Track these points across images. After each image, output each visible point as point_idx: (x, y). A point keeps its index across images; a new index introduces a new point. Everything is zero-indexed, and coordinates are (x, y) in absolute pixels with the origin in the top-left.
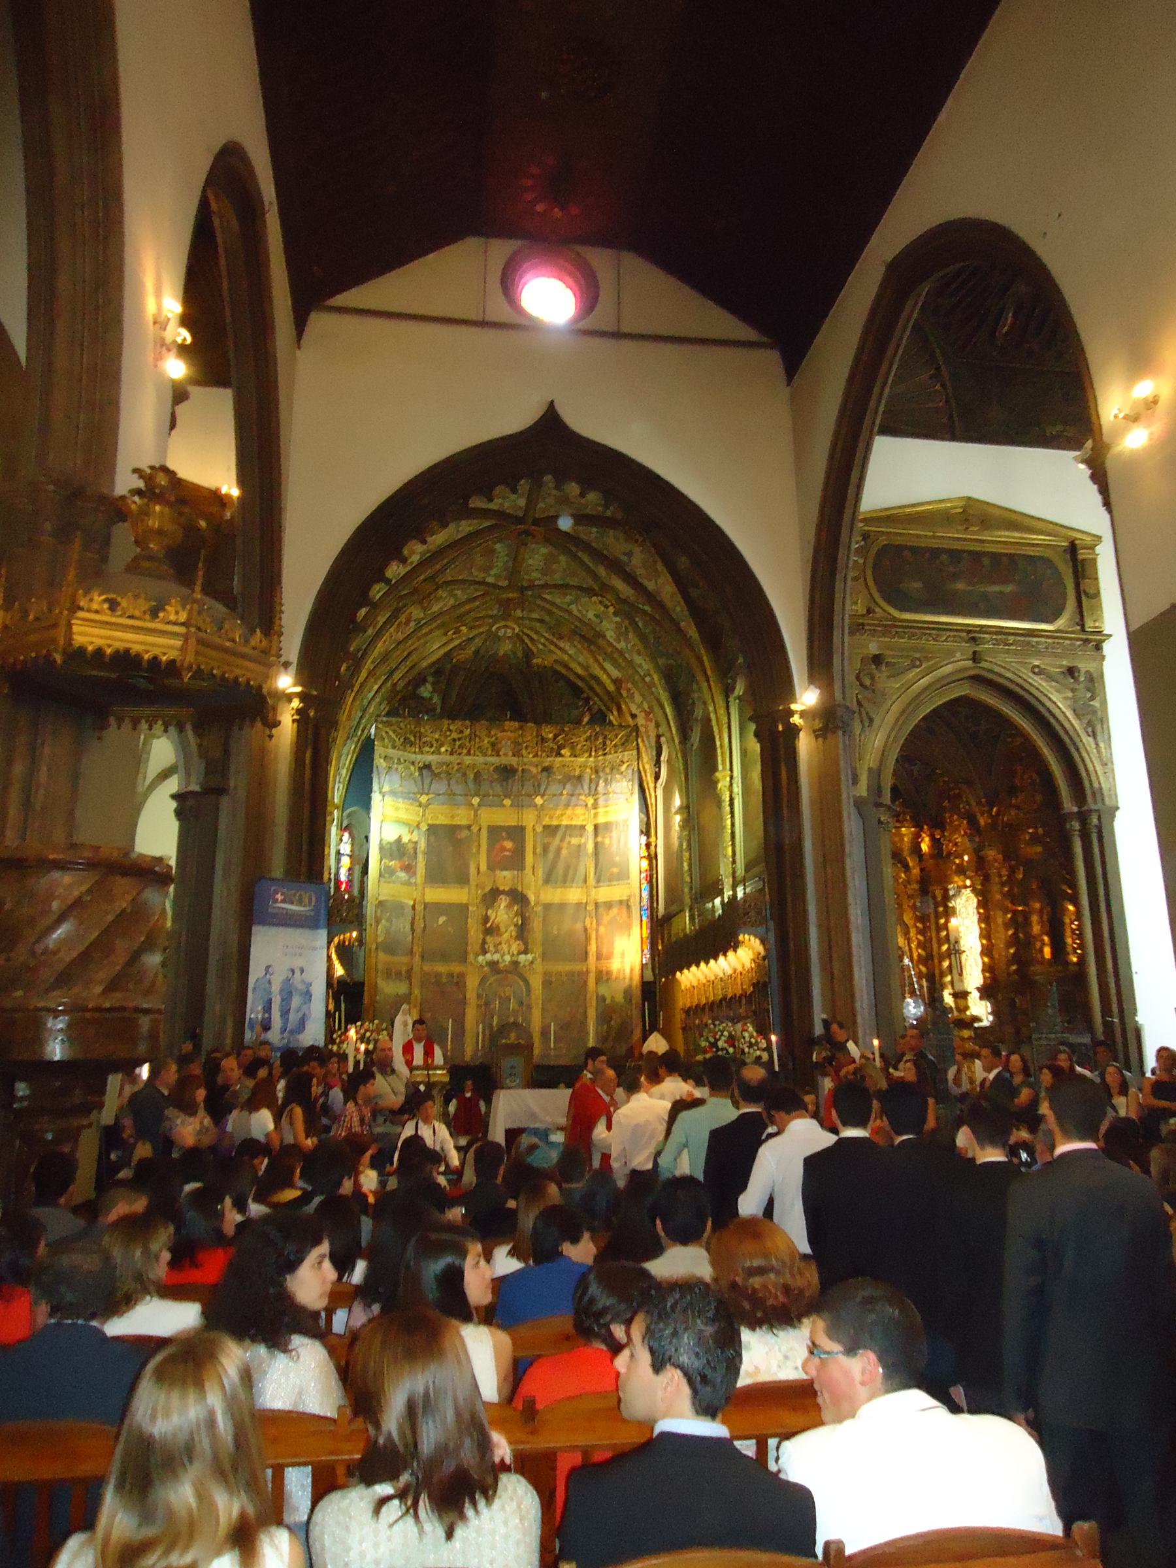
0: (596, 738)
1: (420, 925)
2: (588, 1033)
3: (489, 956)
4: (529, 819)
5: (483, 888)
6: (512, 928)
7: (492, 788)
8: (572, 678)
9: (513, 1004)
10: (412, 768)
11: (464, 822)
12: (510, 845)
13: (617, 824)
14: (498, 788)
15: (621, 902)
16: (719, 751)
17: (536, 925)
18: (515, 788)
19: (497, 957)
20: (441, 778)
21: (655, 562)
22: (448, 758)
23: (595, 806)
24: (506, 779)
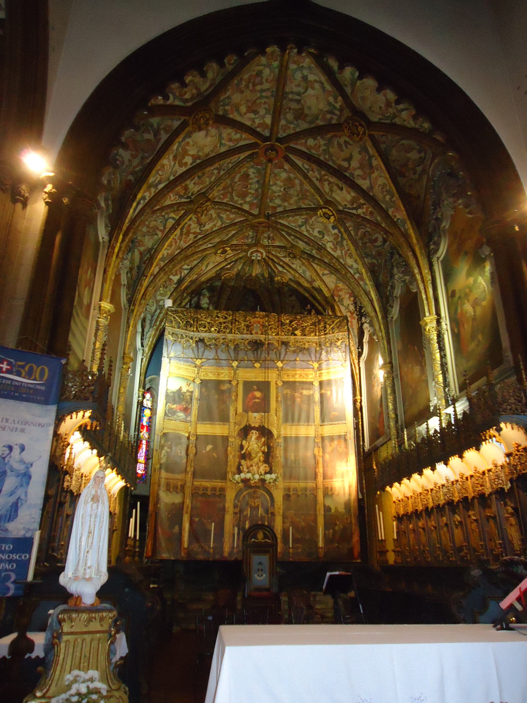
0: (319, 324)
1: (192, 450)
2: (318, 536)
3: (243, 475)
4: (272, 376)
5: (239, 425)
6: (261, 454)
7: (246, 354)
8: (301, 290)
9: (261, 511)
10: (191, 341)
11: (227, 379)
12: (259, 396)
13: (336, 381)
14: (251, 356)
15: (340, 436)
16: (425, 302)
17: (279, 453)
18: (263, 355)
19: (249, 476)
20: (211, 348)
21: (370, 157)
22: (216, 335)
23: (320, 368)
24: (256, 350)
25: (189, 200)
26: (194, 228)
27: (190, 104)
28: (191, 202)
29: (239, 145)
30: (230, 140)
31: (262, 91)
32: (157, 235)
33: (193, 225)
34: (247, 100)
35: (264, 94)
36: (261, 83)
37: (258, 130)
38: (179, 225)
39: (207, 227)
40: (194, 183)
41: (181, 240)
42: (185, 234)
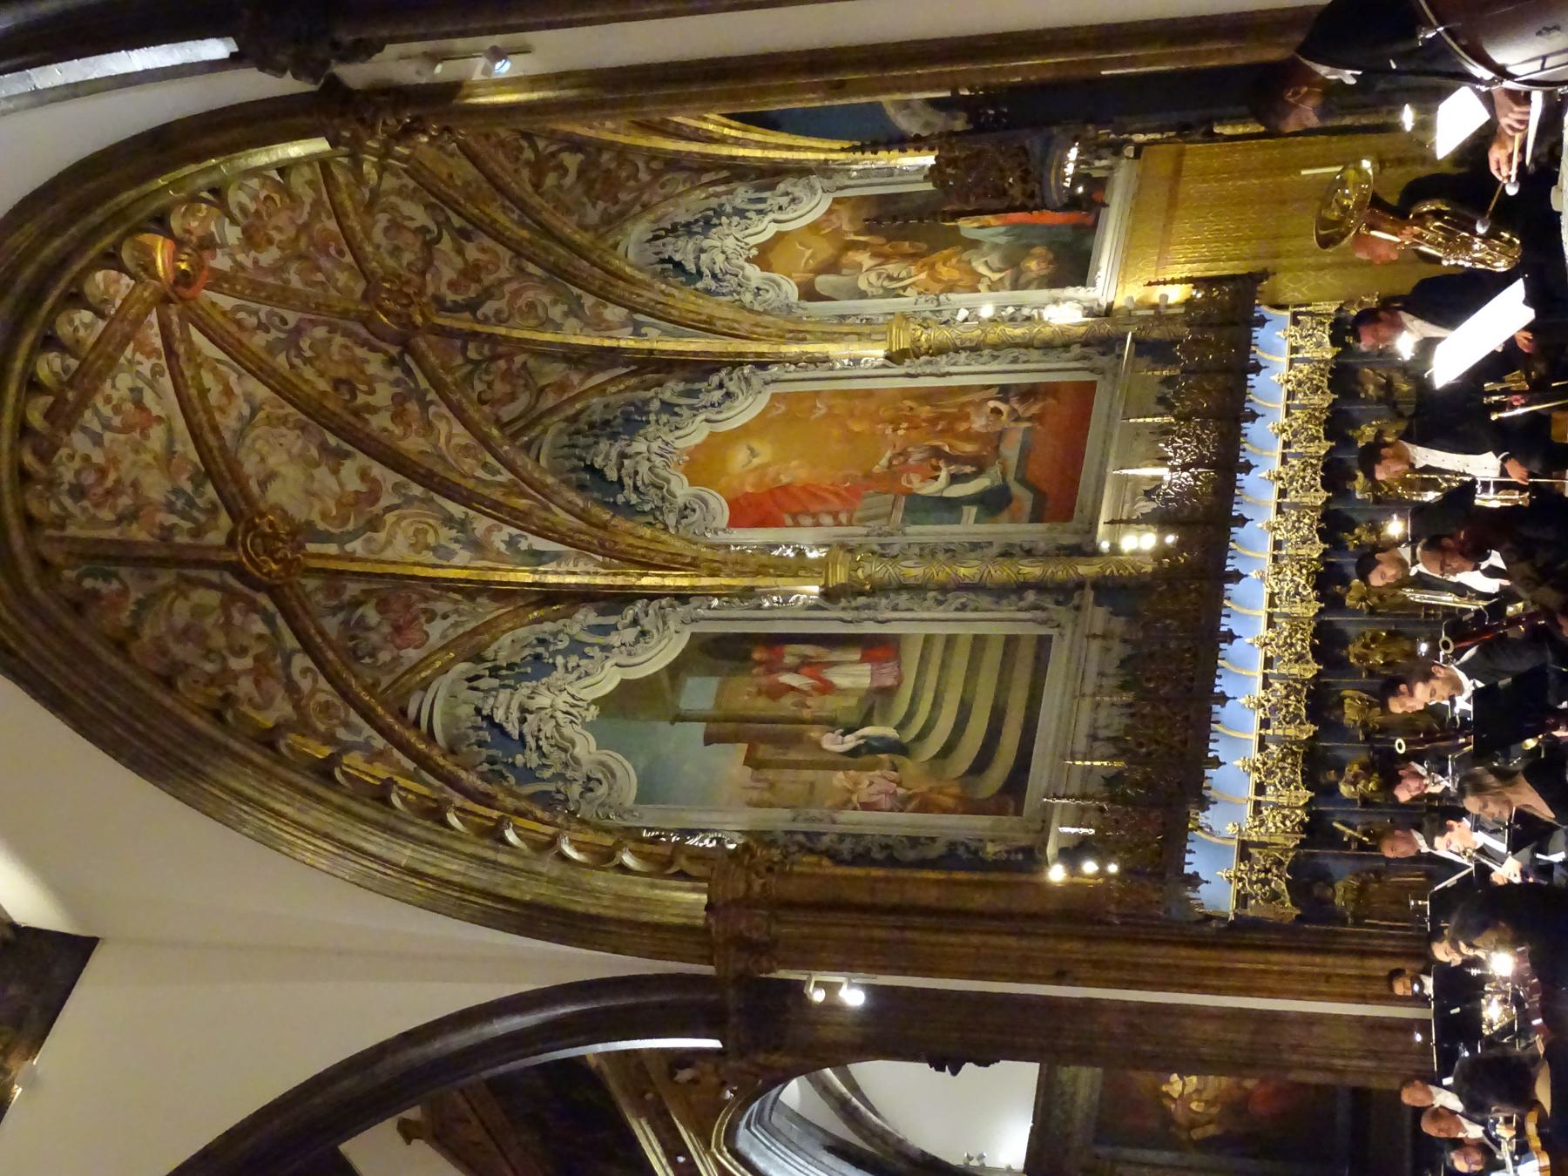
25: (408, 359)
26: (448, 262)
27: (264, 600)
28: (407, 347)
29: (221, 355)
30: (228, 392)
31: (97, 441)
32: (525, 364)
33: (448, 274)
34: (137, 452)
35: (96, 426)
36: (87, 459)
37: (158, 342)
38: (475, 335)
39: (418, 215)
40: (372, 392)
41: (501, 282)
42: (479, 281)
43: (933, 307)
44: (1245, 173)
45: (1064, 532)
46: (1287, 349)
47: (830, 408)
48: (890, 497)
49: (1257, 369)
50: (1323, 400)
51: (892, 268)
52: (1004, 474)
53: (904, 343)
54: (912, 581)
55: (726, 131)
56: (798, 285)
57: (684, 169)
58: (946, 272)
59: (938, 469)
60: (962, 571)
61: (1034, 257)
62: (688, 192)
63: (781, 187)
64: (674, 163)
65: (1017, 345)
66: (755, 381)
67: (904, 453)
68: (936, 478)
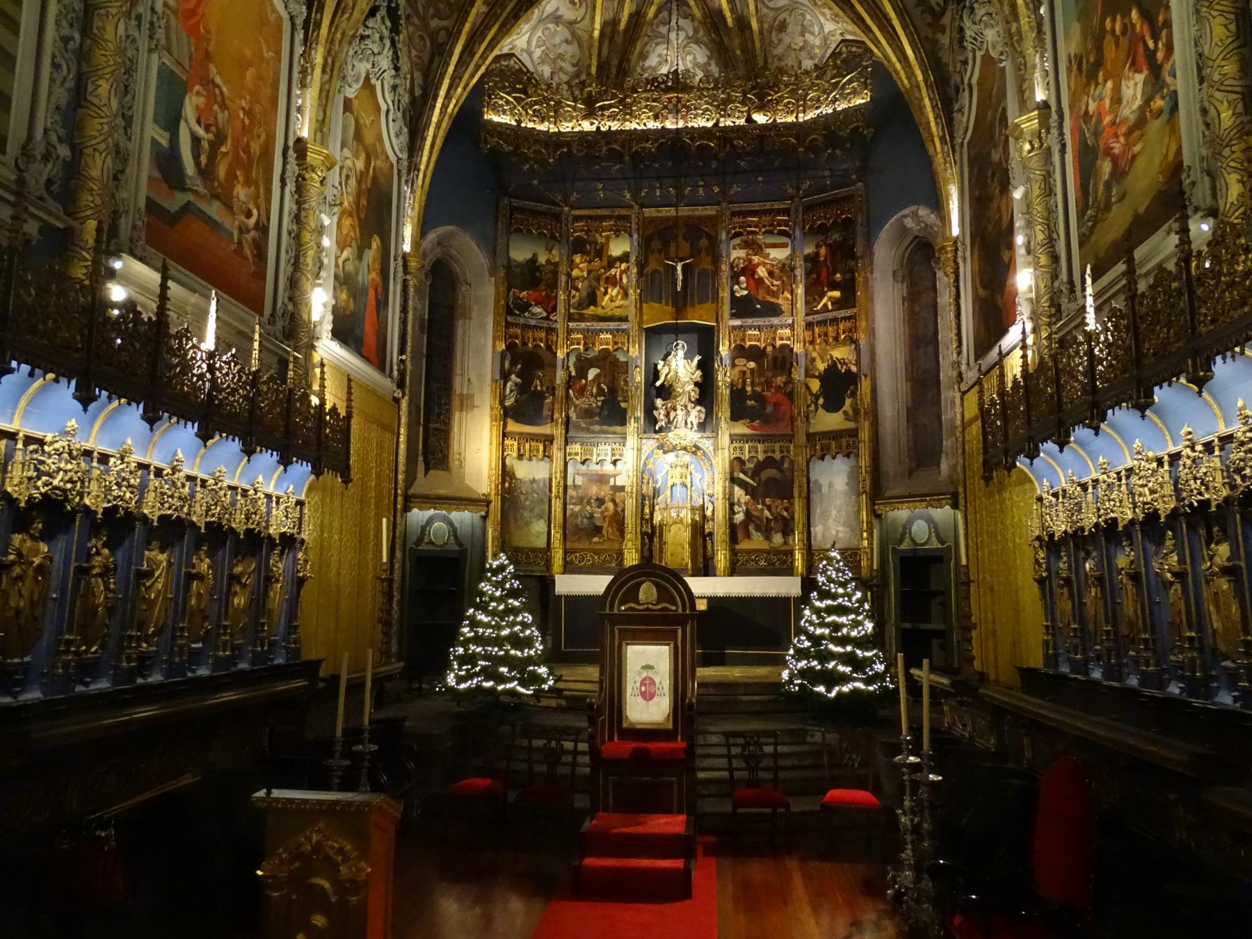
43: (329, 199)
44: (378, 476)
45: (134, 227)
46: (281, 493)
47: (268, 62)
48: (187, 65)
49: (285, 462)
50: (238, 523)
51: (353, 182)
52: (196, 193)
53: (312, 158)
54: (97, 23)
55: (454, 101)
56: (350, 100)
57: (431, 62)
58: (347, 222)
59: (207, 129)
60: (104, 86)
61: (349, 298)
62: (410, 57)
63: (406, 130)
64: (440, 51)
65: (297, 258)
66: (297, 6)
67: (224, 106)
68: (198, 122)
